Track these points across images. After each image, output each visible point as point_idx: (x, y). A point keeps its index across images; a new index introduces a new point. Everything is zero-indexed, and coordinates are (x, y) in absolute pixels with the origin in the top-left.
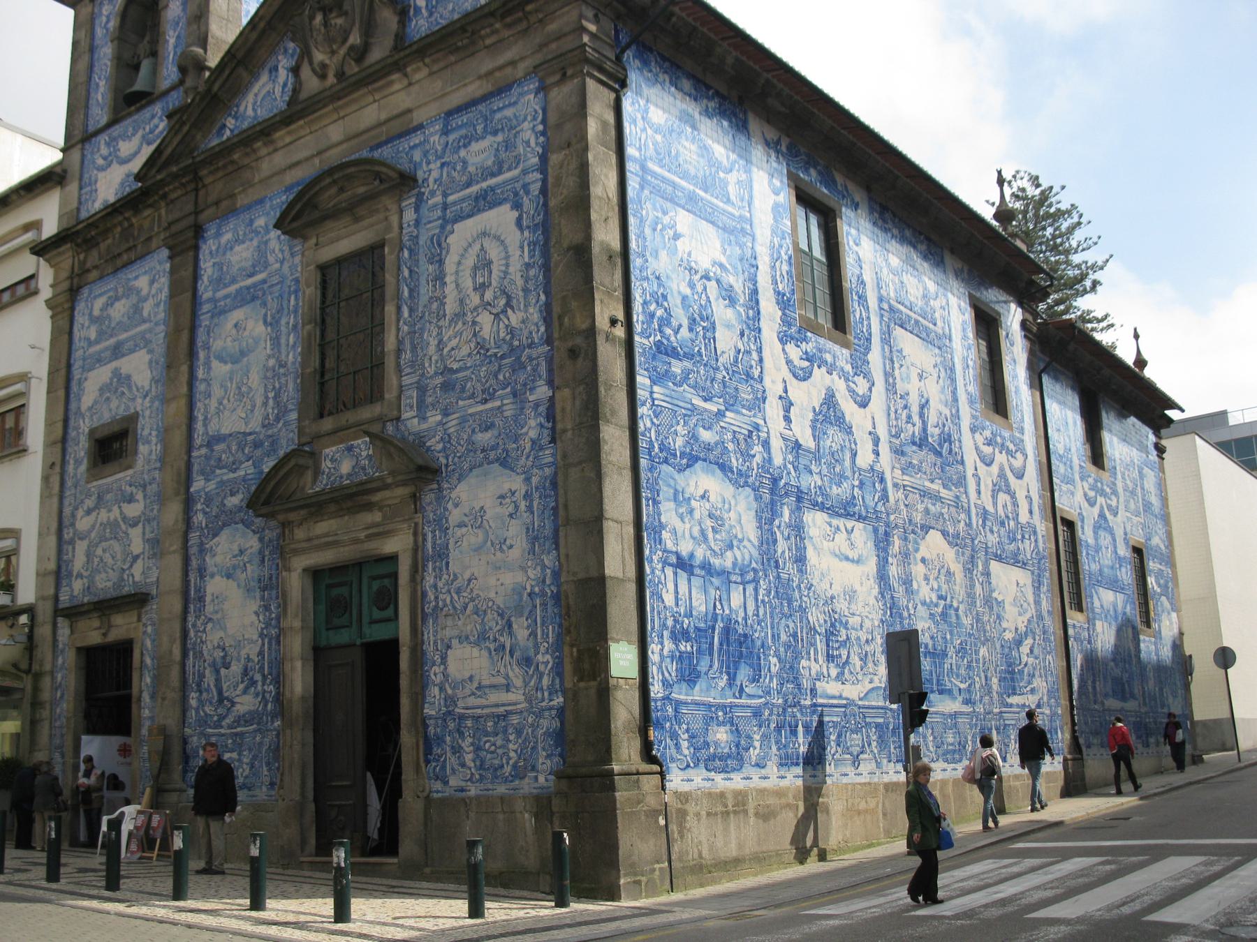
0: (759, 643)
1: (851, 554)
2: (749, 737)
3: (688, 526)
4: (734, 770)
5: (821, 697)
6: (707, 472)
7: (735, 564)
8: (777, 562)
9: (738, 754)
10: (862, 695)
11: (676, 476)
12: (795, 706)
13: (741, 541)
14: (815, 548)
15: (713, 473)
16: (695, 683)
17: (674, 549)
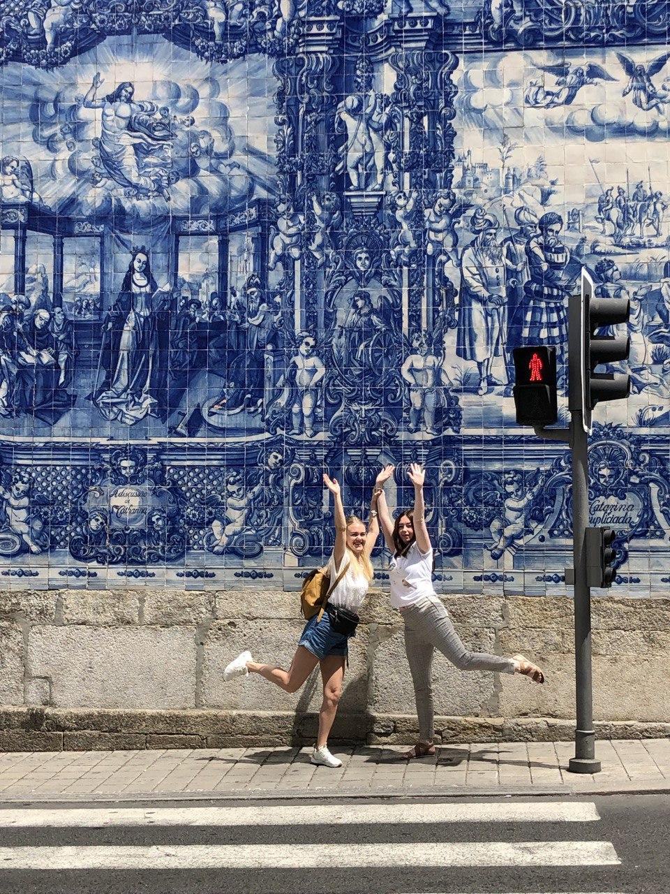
0: (264, 334)
1: (642, 119)
2: (212, 502)
3: (65, 154)
4: (156, 559)
5: (473, 423)
6: (132, 49)
7: (196, 204)
8: (341, 182)
9: (173, 531)
10: (650, 415)
11: (40, 75)
12: (374, 443)
13: (220, 157)
14: (489, 129)
15: (149, 49)
16: (57, 416)
17: (23, 199)
